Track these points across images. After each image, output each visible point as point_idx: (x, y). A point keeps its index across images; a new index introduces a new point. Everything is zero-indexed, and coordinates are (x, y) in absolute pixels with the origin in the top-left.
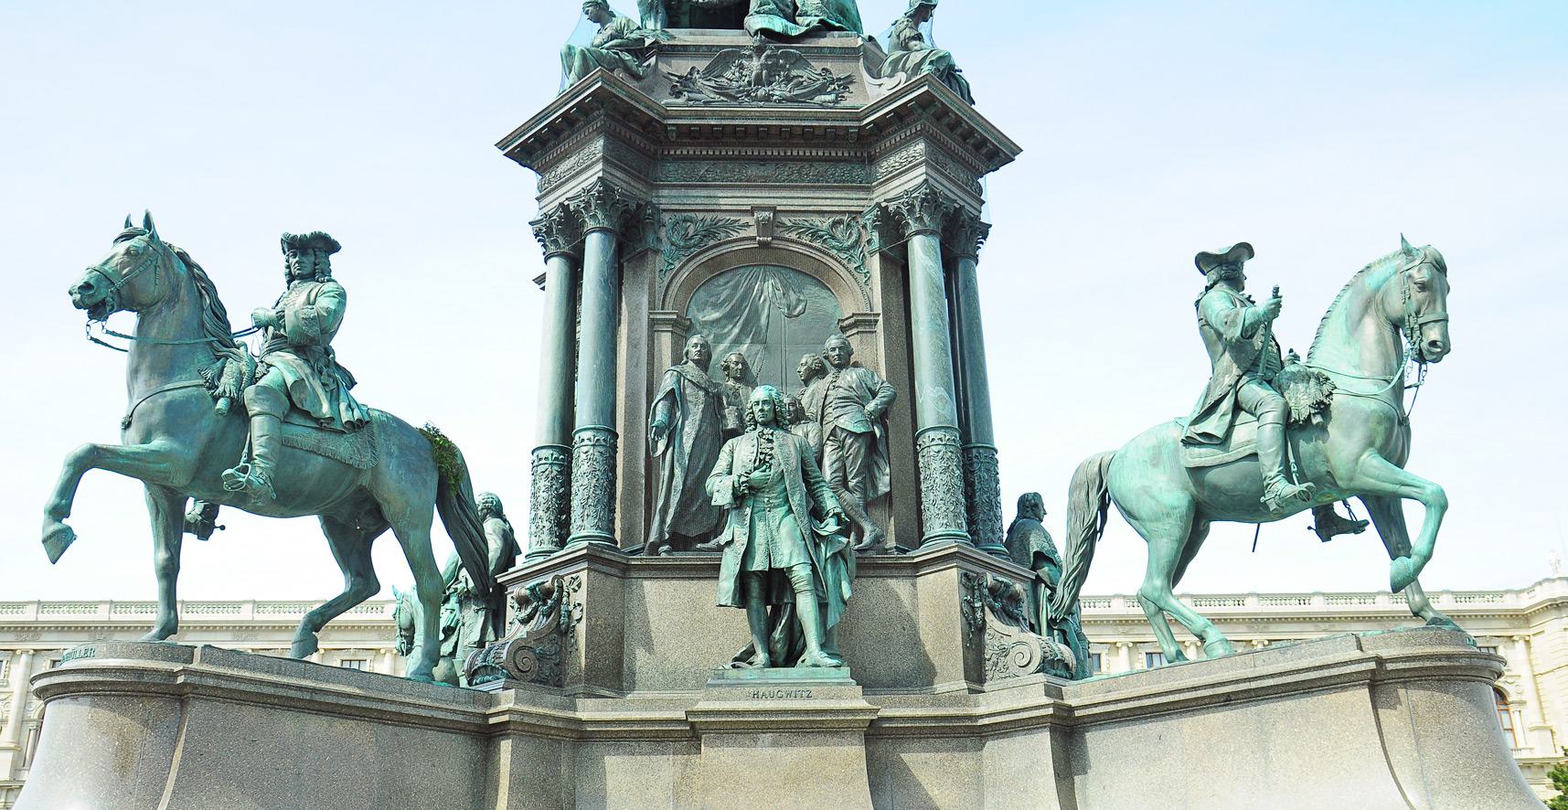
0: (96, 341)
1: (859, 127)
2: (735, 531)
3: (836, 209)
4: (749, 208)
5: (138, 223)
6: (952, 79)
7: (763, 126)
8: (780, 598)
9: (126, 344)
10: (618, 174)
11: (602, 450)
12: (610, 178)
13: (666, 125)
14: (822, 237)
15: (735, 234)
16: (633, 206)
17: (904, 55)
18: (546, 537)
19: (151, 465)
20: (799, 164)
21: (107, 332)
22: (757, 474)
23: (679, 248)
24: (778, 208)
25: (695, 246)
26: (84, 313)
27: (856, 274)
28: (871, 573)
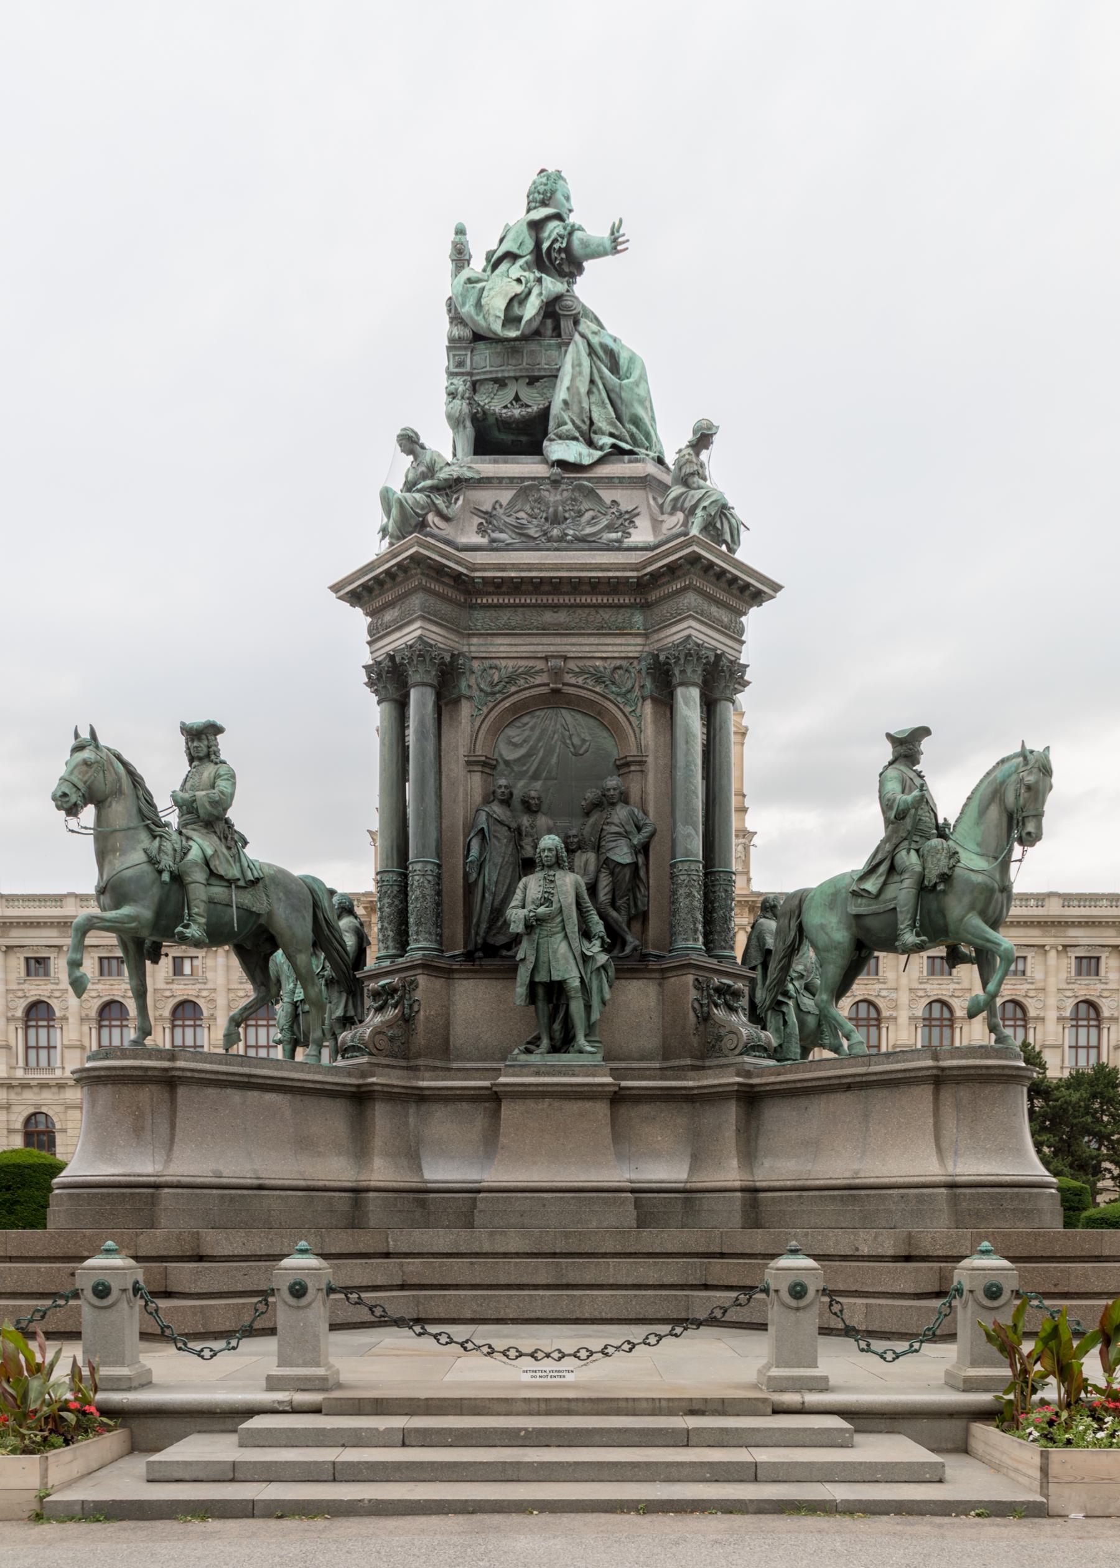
0: (73, 831)
1: (638, 578)
2: (524, 950)
3: (616, 655)
4: (544, 655)
5: (85, 735)
6: (724, 520)
7: (555, 578)
8: (558, 999)
9: (92, 832)
10: (434, 628)
11: (430, 878)
12: (428, 634)
13: (473, 578)
14: (604, 682)
15: (532, 680)
17: (682, 494)
18: (390, 944)
19: (126, 925)
20: (587, 610)
21: (82, 827)
22: (542, 909)
23: (487, 694)
24: (569, 655)
25: (500, 692)
26: (63, 813)
28: (628, 975)
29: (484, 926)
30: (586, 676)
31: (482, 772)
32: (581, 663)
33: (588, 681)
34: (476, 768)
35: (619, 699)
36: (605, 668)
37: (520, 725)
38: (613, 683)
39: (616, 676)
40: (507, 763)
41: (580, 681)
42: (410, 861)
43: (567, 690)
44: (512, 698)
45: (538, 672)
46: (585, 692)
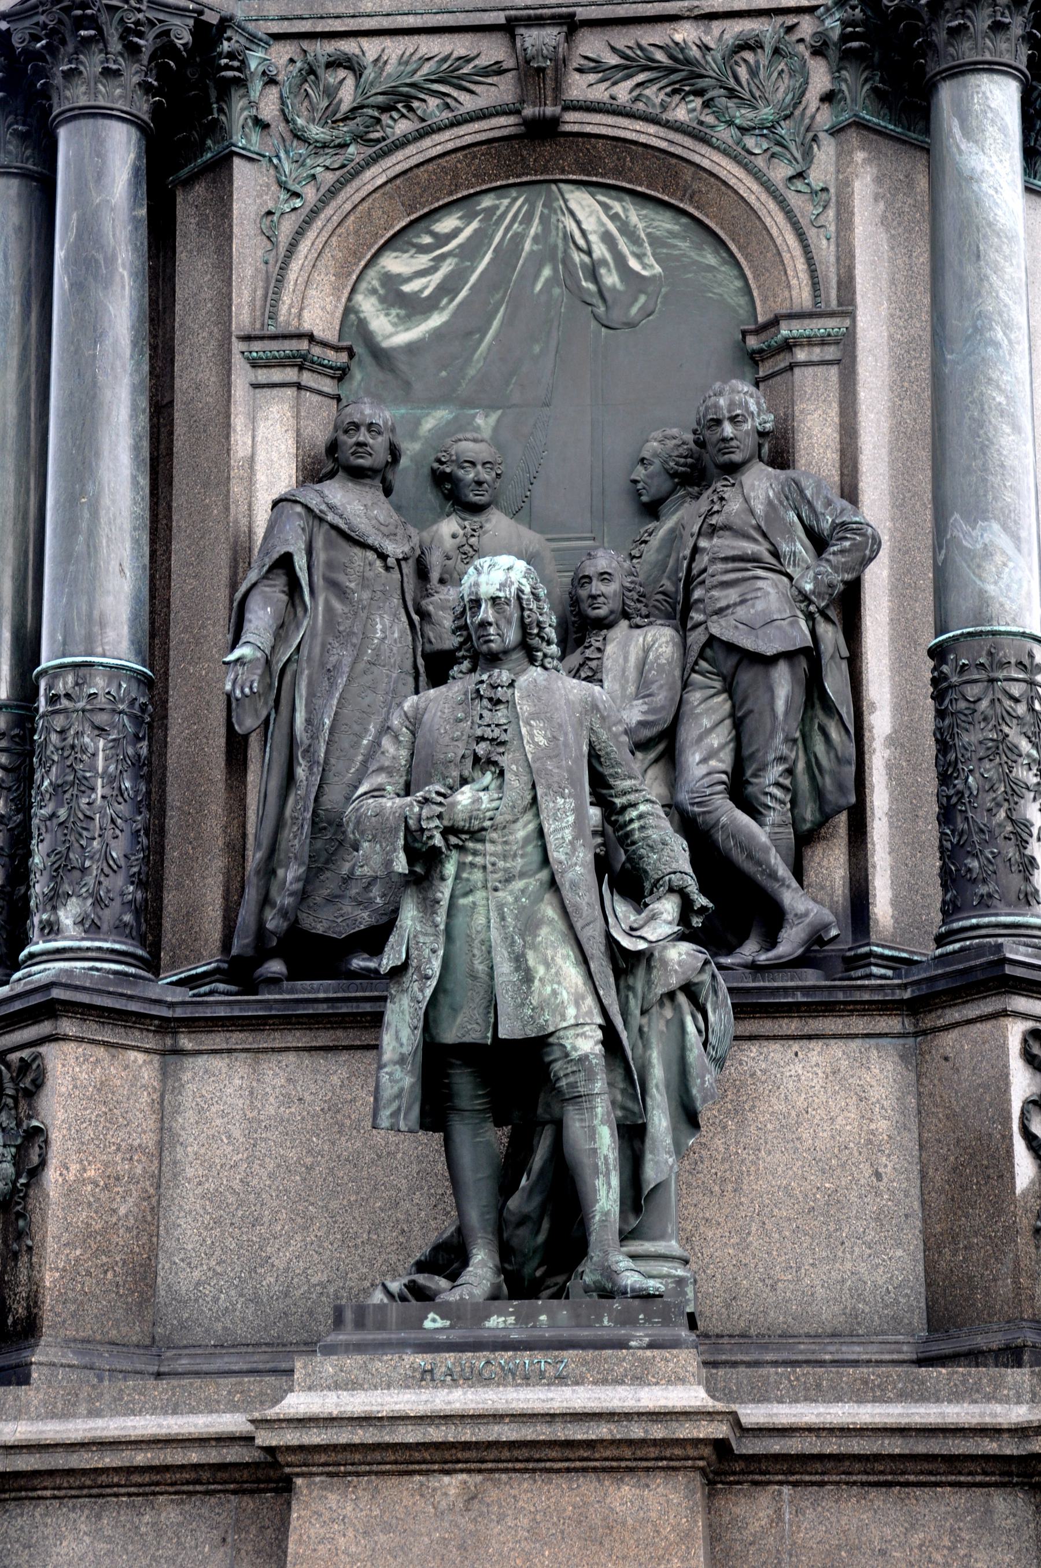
15: (463, 97)
16: (183, 35)
27: (794, 200)
29: (291, 874)
30: (641, 77)
31: (299, 386)
32: (624, 38)
33: (650, 92)
34: (277, 375)
35: (750, 142)
36: (705, 48)
37: (427, 240)
38: (732, 94)
39: (743, 72)
40: (380, 356)
41: (623, 92)
42: (44, 664)
43: (574, 122)
44: (400, 155)
45: (487, 72)
46: (639, 125)
